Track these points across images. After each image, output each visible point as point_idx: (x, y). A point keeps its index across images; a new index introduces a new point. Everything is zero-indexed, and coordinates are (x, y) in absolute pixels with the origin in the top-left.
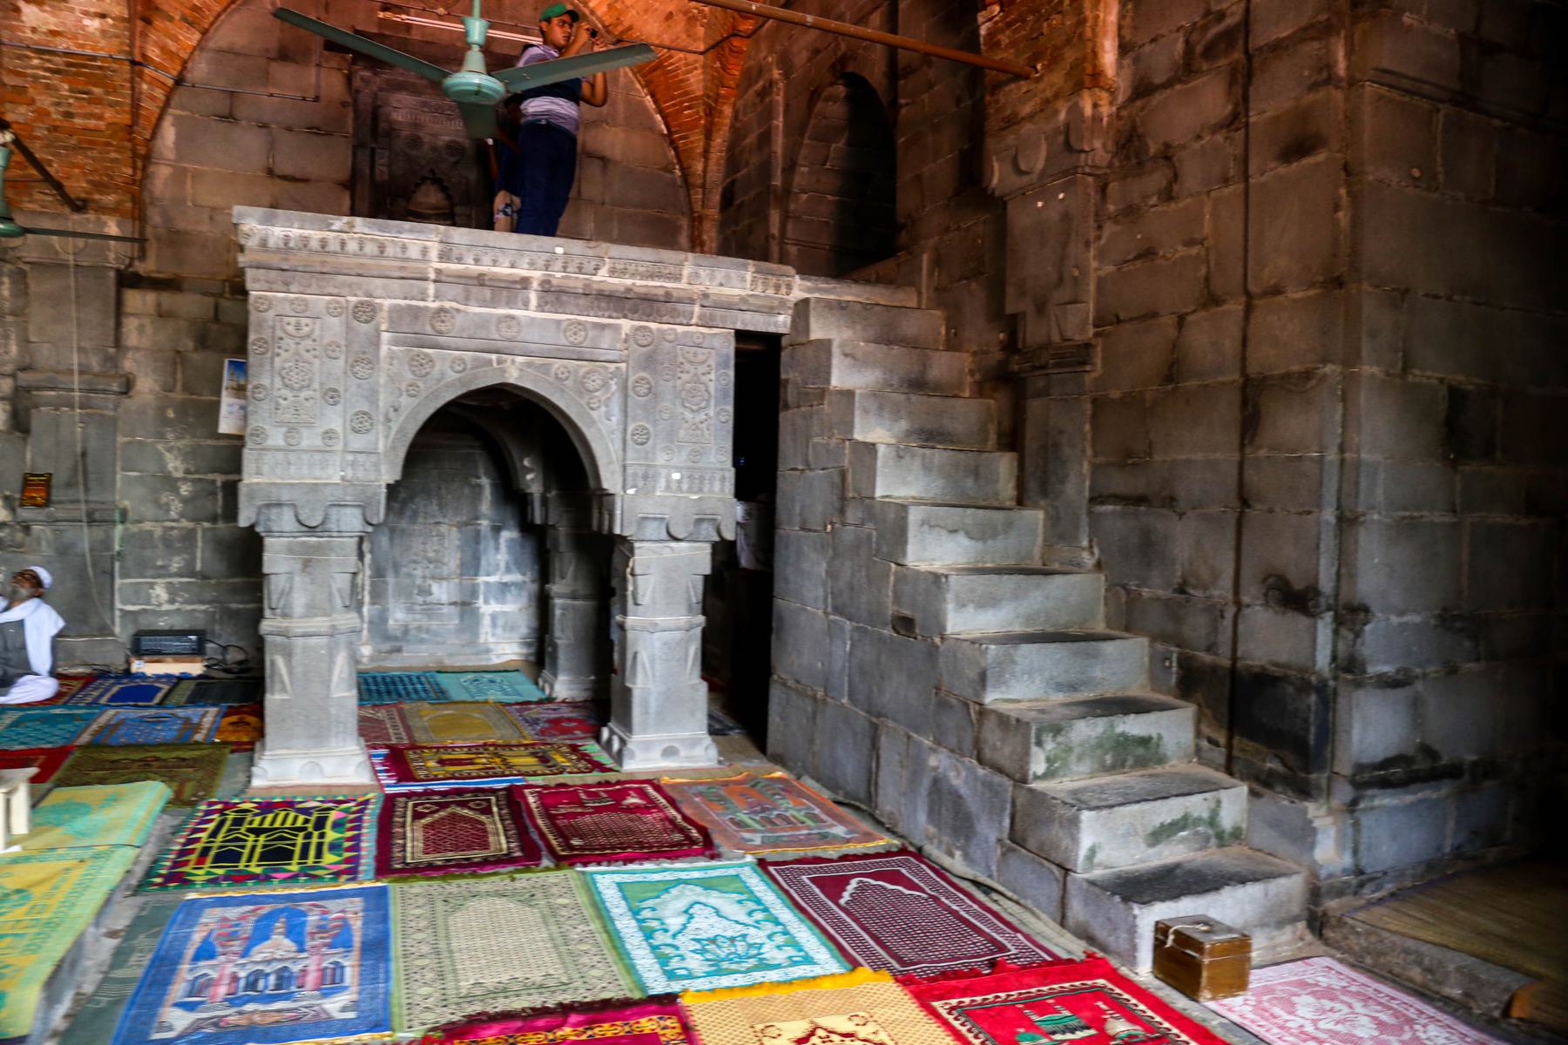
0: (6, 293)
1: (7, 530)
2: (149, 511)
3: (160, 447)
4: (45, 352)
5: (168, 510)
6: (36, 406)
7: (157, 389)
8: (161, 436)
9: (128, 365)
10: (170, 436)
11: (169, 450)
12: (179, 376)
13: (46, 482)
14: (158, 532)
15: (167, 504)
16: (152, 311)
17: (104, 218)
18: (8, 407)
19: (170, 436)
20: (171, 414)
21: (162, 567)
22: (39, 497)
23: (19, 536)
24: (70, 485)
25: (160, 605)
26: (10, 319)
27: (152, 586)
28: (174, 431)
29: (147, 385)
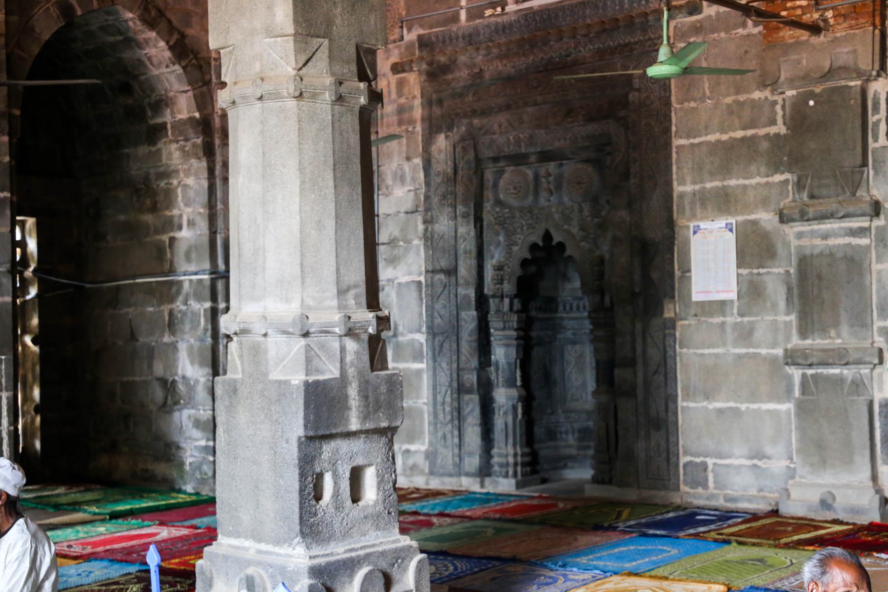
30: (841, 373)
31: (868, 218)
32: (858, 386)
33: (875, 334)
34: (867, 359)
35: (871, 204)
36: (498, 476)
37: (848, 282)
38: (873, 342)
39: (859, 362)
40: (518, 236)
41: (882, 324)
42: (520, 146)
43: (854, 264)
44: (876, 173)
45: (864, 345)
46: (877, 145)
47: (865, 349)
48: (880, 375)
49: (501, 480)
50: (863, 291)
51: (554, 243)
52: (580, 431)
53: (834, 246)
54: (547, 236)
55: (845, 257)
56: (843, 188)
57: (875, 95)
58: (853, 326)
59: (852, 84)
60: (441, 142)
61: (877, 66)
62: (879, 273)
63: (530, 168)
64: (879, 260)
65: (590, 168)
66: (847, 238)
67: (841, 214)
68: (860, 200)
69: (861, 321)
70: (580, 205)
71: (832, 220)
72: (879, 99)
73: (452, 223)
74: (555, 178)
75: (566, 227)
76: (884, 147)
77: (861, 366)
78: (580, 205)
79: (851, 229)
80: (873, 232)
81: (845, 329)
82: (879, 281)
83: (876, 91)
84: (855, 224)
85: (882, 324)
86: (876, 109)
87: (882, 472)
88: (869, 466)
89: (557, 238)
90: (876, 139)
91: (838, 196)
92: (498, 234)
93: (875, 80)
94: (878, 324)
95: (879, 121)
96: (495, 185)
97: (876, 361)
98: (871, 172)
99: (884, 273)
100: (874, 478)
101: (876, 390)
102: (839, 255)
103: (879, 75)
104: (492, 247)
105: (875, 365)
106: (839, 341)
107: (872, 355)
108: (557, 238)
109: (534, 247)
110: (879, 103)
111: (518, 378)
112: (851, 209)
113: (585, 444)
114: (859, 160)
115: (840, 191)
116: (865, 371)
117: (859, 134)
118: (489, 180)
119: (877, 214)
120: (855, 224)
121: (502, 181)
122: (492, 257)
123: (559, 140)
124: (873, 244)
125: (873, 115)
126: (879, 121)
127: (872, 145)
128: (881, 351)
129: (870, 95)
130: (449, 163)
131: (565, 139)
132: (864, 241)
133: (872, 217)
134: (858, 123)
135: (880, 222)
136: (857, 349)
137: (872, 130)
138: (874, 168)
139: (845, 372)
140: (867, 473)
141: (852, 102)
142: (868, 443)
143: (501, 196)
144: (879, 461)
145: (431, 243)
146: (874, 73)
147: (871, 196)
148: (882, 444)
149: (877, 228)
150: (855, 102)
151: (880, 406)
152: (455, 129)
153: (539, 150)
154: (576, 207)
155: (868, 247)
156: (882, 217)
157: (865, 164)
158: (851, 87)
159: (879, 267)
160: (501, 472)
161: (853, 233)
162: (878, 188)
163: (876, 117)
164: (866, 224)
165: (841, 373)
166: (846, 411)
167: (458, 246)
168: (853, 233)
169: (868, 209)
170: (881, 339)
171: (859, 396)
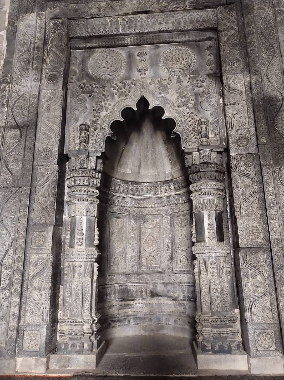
36: (69, 353)
40: (108, 103)
42: (117, 29)
49: (75, 356)
51: (150, 108)
52: (119, 292)
54: (143, 102)
60: (32, 20)
63: (123, 49)
65: (188, 50)
70: (179, 78)
73: (37, 84)
74: (151, 57)
75: (162, 95)
78: (179, 78)
89: (153, 104)
92: (85, 101)
96: (84, 61)
104: (77, 112)
108: (153, 104)
109: (127, 112)
111: (96, 237)
113: (124, 303)
118: (76, 58)
121: (91, 59)
122: (77, 120)
123: (160, 24)
130: (38, 35)
131: (167, 23)
143: (90, 71)
145: (7, 102)
152: (48, 10)
153: (137, 31)
154: (174, 79)
160: (74, 345)
167: (41, 105)
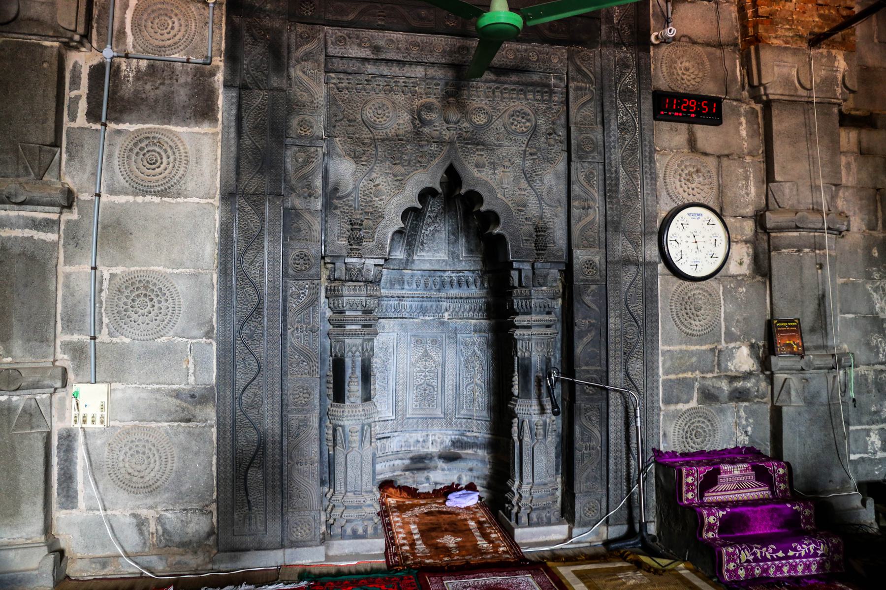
0: (744, 133)
1: (753, 380)
2: (862, 354)
3: (868, 287)
4: (787, 191)
5: (878, 353)
6: (777, 249)
7: (864, 228)
8: (869, 276)
9: (841, 204)
10: (876, 276)
11: (876, 290)
12: (880, 214)
13: (796, 328)
14: (871, 376)
15: (877, 347)
16: (856, 150)
17: (834, 52)
18: (751, 250)
19: (876, 276)
20: (875, 253)
21: (875, 412)
22: (795, 342)
23: (763, 385)
24: (813, 330)
25: (875, 453)
26: (748, 159)
27: (868, 432)
28: (879, 270)
29: (857, 223)
30: (9, 400)
31: (57, 209)
32: (32, 415)
33: (58, 350)
34: (47, 382)
35: (62, 191)
37: (26, 286)
38: (55, 361)
39: (35, 386)
41: (67, 338)
43: (36, 264)
44: (71, 157)
45: (43, 365)
46: (73, 125)
47: (45, 369)
48: (62, 400)
50: (46, 298)
53: (9, 238)
55: (23, 254)
56: (26, 168)
57: (74, 67)
58: (29, 340)
59: (47, 43)
61: (81, 29)
62: (67, 276)
64: (68, 261)
66: (27, 230)
67: (21, 199)
68: (48, 184)
69: (40, 333)
71: (7, 206)
72: (80, 73)
76: (83, 129)
77: (38, 391)
79: (34, 220)
80: (62, 227)
81: (17, 346)
82: (67, 286)
83: (76, 63)
84: (39, 214)
85: (67, 338)
86: (75, 83)
87: (58, 518)
88: (42, 516)
90: (73, 118)
91: (18, 176)
93: (77, 49)
94: (62, 337)
95: (78, 97)
97: (58, 384)
98: (64, 156)
99: (73, 276)
100: (47, 529)
101: (55, 420)
102: (16, 250)
103: (81, 43)
105: (56, 389)
106: (9, 359)
107: (52, 377)
110: (80, 78)
112: (36, 195)
114: (50, 138)
115: (22, 171)
116: (42, 396)
117: (52, 104)
119: (69, 207)
120: (39, 214)
124: (62, 242)
125: (71, 90)
126: (78, 97)
127: (67, 123)
128: (65, 371)
129: (69, 66)
132: (51, 237)
133: (63, 207)
134: (52, 93)
135: (73, 216)
136: (34, 370)
137: (69, 107)
138: (68, 151)
139: (15, 398)
140: (39, 525)
141: (45, 65)
142: (42, 487)
144: (55, 505)
146: (77, 37)
147: (63, 184)
148: (60, 484)
149: (68, 222)
150: (49, 67)
151: (60, 438)
155: (55, 245)
156: (75, 210)
157: (57, 144)
158: (46, 47)
159: (68, 269)
161: (36, 225)
162: (72, 177)
163: (74, 93)
164: (55, 217)
165: (9, 400)
166: (13, 448)
168: (36, 225)
169: (60, 199)
170: (66, 357)
171: (32, 428)
